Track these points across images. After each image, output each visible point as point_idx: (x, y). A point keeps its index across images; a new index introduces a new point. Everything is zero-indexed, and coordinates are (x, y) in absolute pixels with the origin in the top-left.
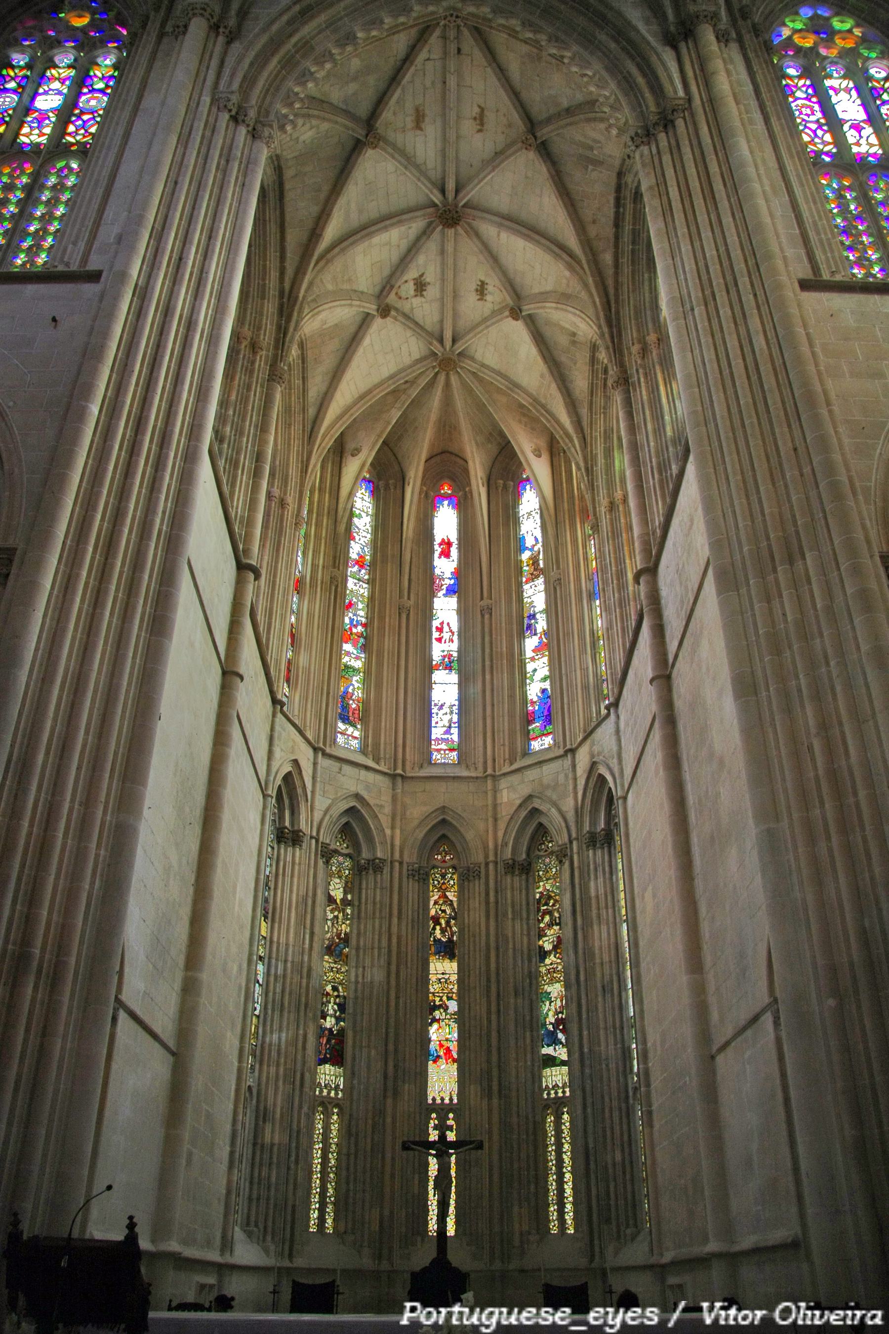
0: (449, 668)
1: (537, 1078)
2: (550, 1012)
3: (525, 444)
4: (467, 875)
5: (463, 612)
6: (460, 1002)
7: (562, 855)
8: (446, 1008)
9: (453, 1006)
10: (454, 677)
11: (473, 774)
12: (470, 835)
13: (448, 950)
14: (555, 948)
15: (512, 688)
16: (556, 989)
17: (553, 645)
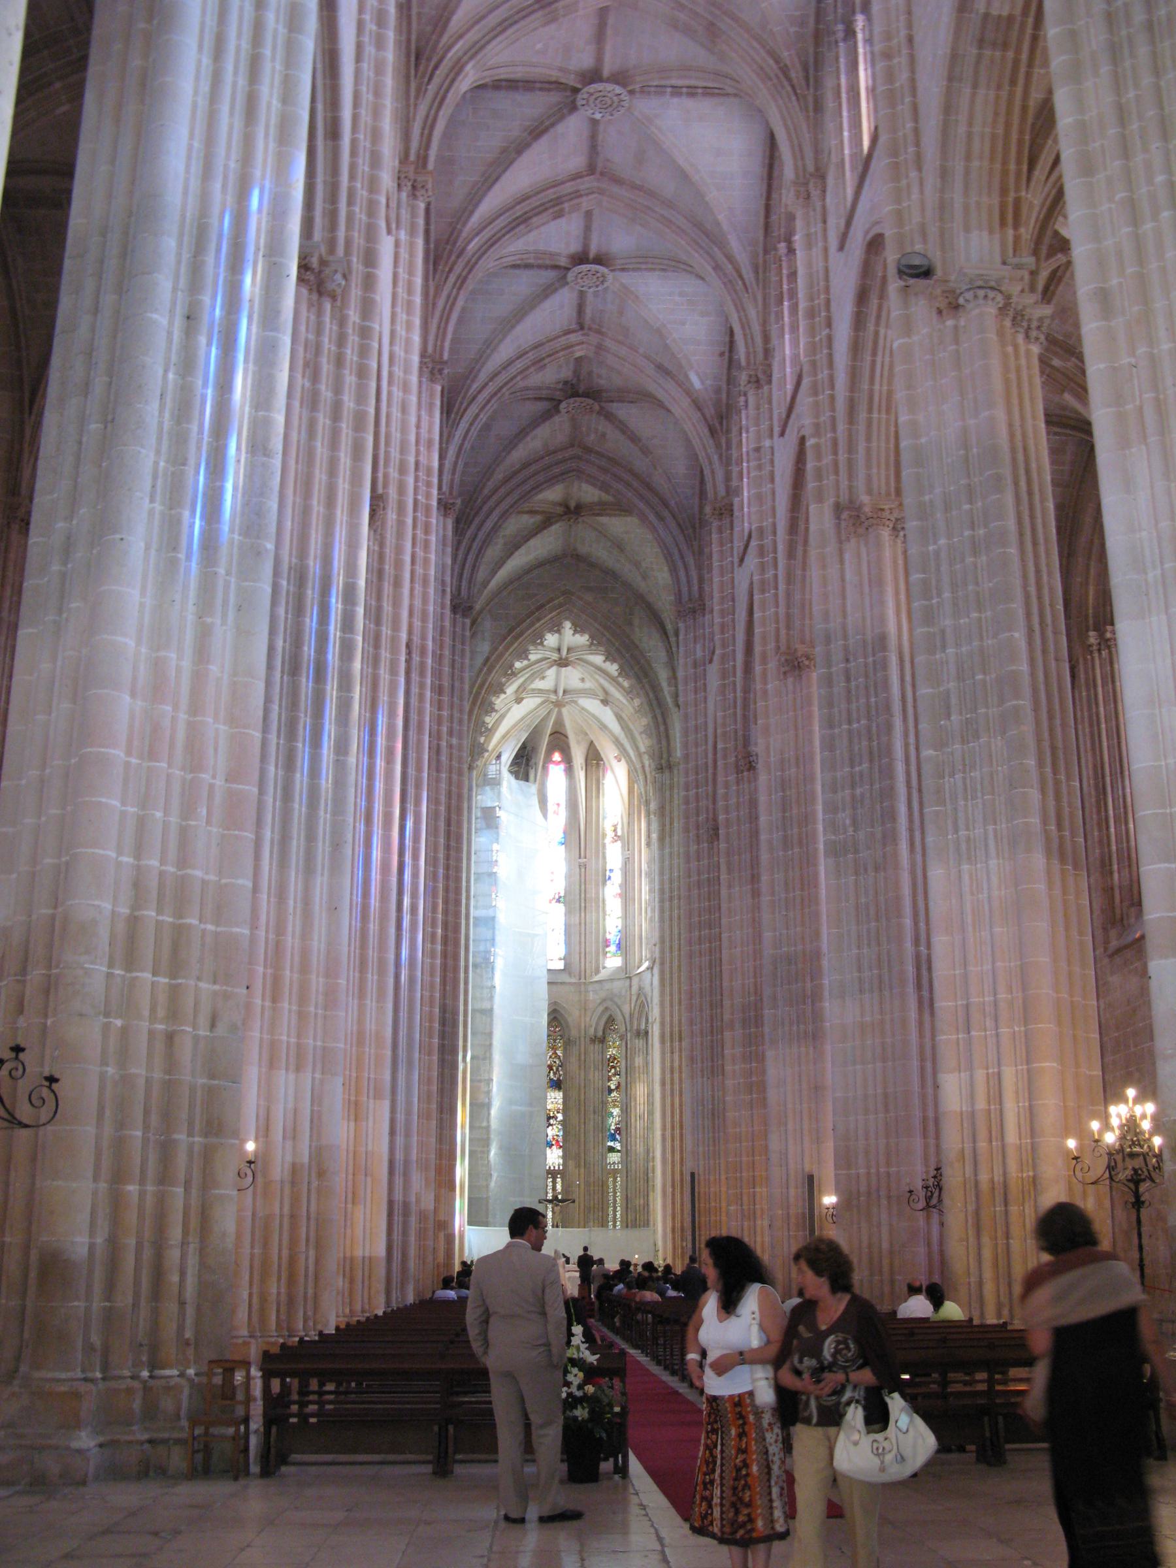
0: (558, 901)
1: (604, 1158)
2: (612, 1123)
3: (609, 752)
4: (568, 1043)
5: (569, 861)
6: (564, 1115)
7: (622, 1038)
8: (555, 1117)
9: (560, 1117)
10: (561, 908)
11: (573, 980)
12: (570, 1020)
13: (557, 1085)
14: (618, 1087)
15: (598, 922)
16: (616, 1111)
17: (627, 895)
